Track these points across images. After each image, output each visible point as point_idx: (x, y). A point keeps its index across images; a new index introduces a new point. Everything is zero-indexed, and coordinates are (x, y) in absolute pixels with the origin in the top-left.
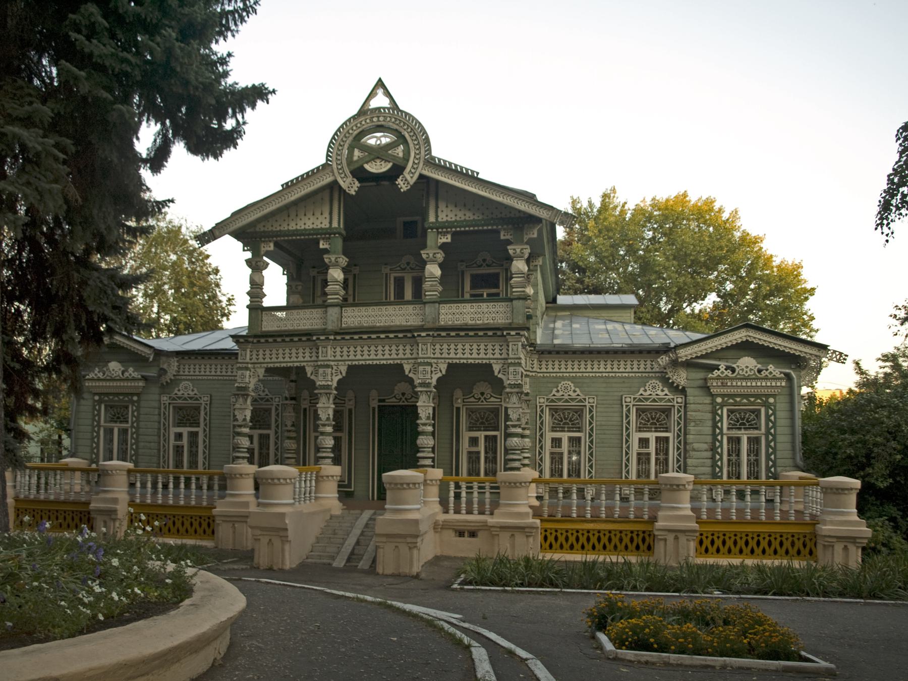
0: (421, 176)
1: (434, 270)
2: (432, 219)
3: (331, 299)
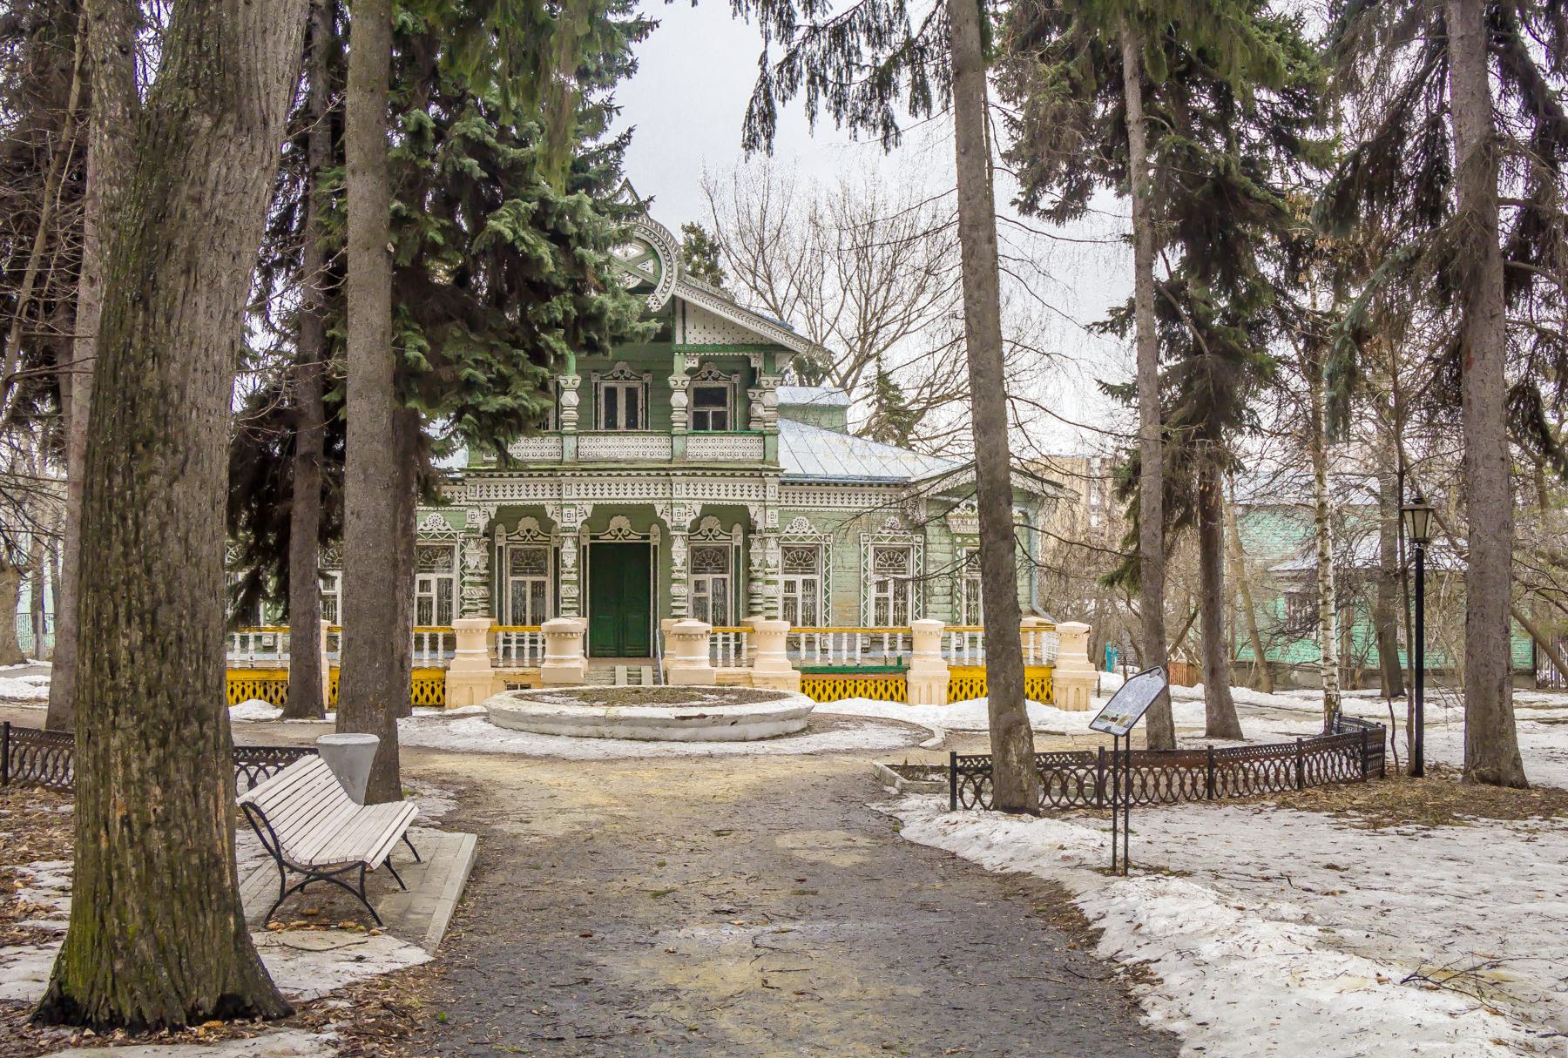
0: (674, 298)
1: (680, 399)
2: (679, 341)
3: (569, 427)
